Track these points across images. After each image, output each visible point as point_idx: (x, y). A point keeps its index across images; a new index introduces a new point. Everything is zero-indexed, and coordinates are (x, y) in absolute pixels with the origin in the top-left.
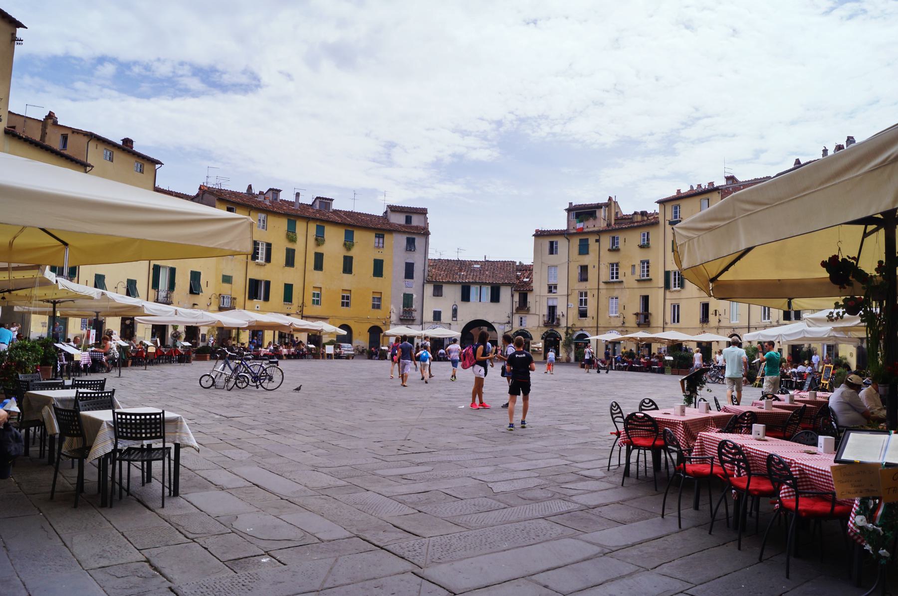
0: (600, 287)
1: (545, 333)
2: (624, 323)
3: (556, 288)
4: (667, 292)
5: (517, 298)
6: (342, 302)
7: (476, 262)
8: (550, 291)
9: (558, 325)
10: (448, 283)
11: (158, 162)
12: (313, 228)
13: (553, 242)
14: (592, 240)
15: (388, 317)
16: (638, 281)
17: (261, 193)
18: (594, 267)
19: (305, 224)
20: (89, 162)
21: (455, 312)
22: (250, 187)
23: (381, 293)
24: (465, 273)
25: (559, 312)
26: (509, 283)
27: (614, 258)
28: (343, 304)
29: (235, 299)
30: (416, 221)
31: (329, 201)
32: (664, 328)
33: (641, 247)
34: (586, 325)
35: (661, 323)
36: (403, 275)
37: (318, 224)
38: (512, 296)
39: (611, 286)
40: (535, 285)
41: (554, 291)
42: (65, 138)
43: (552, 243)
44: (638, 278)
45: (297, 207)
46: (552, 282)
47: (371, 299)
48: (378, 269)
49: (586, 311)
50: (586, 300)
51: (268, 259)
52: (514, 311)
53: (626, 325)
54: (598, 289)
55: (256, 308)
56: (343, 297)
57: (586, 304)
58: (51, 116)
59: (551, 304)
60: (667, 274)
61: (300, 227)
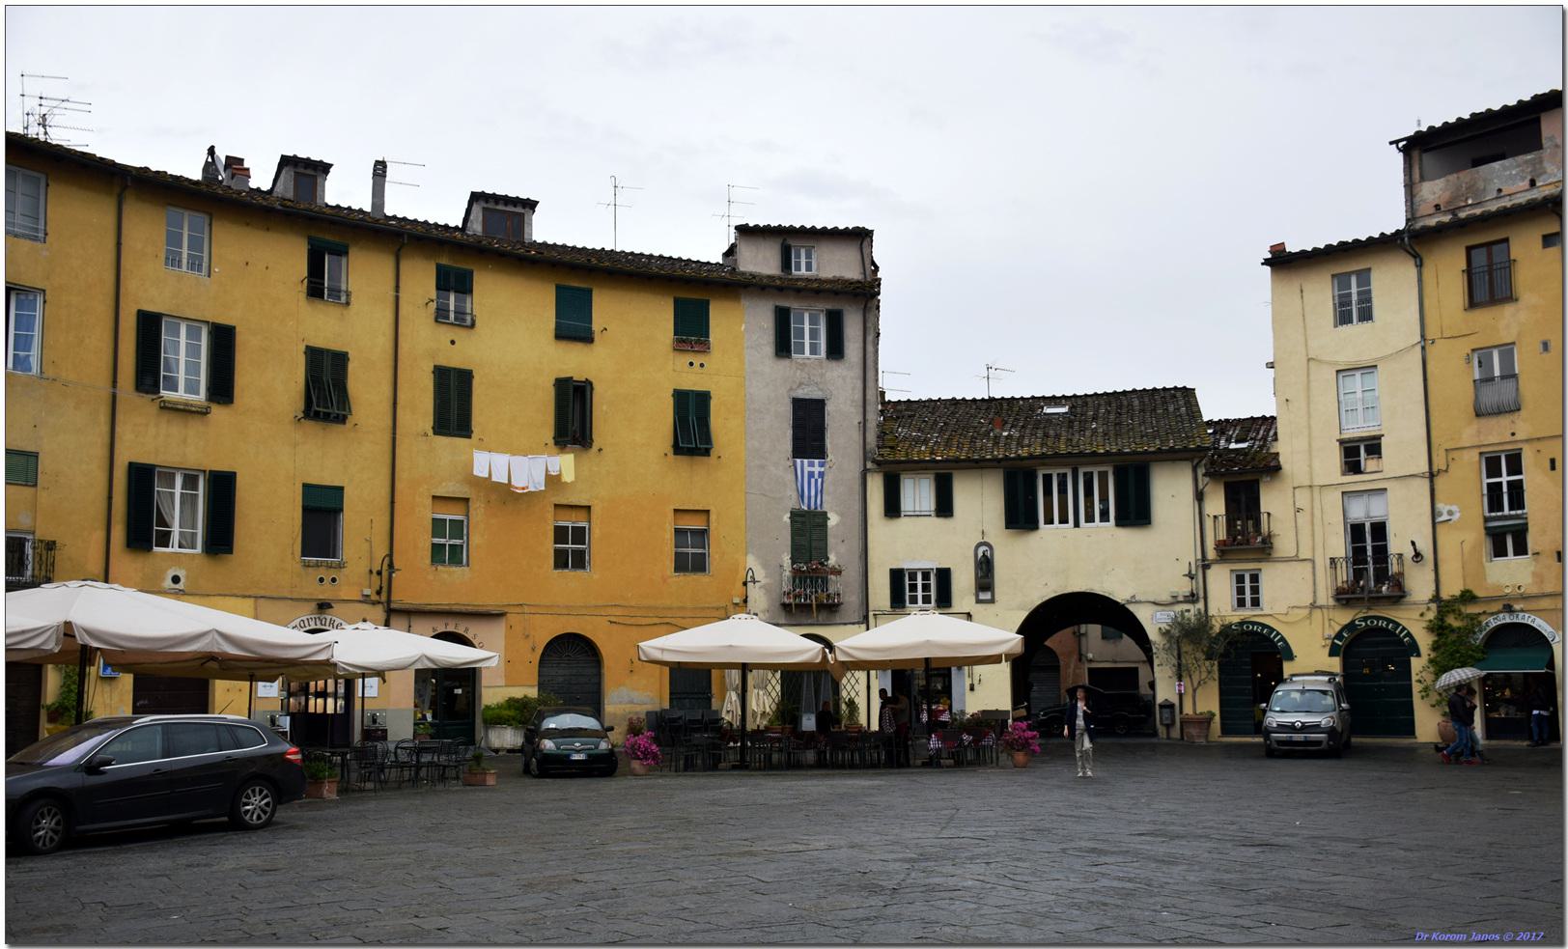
1: (1345, 628)
3: (1374, 447)
6: (557, 552)
7: (1054, 400)
8: (1352, 466)
15: (737, 600)
21: (985, 570)
24: (1015, 433)
25: (1397, 544)
26: (1186, 449)
28: (561, 561)
29: (51, 546)
30: (834, 265)
31: (519, 210)
36: (787, 445)
38: (1199, 497)
40: (1287, 448)
41: (1369, 464)
47: (669, 535)
49: (1527, 524)
50: (1517, 489)
51: (222, 387)
52: (1211, 554)
55: (168, 583)
56: (560, 534)
57: (1517, 500)
59: (1358, 512)
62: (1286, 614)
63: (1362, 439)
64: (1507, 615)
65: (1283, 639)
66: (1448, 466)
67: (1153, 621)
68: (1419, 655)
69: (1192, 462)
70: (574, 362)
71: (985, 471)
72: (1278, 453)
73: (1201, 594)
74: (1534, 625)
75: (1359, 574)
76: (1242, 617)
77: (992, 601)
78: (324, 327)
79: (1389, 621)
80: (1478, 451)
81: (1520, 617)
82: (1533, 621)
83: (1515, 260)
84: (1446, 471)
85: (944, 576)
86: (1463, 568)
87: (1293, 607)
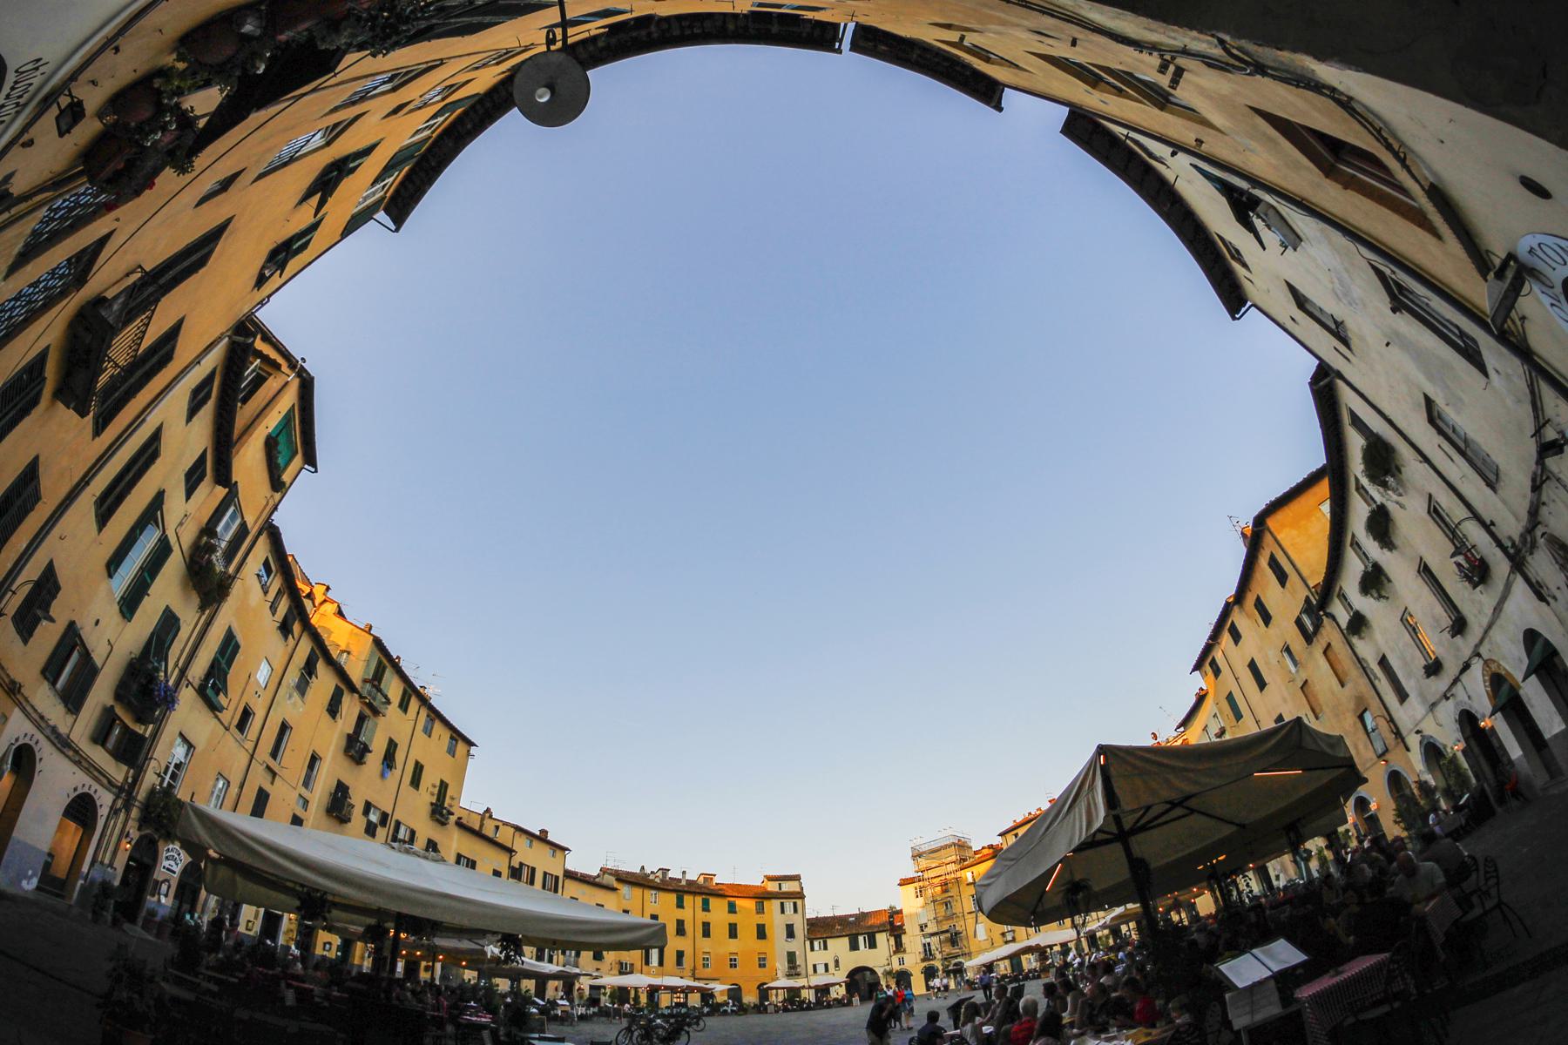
7: (851, 916)
11: (568, 849)
12: (699, 899)
17: (652, 872)
19: (692, 898)
20: (514, 848)
22: (643, 868)
25: (933, 947)
37: (704, 897)
38: (888, 940)
42: (497, 828)
45: (684, 883)
48: (761, 933)
56: (731, 960)
58: (488, 810)
61: (688, 899)
67: (880, 972)
70: (732, 918)
75: (926, 954)
78: (680, 914)
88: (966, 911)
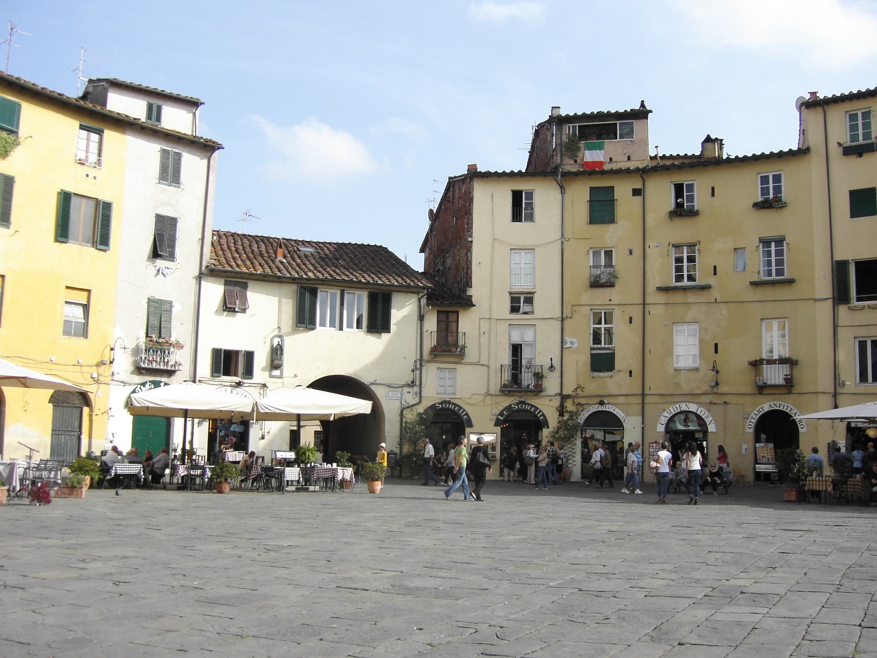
0: (649, 300)
2: (717, 384)
3: (529, 300)
4: (843, 309)
5: (431, 323)
8: (515, 309)
9: (538, 390)
10: (264, 279)
13: (520, 192)
14: (623, 190)
16: (755, 284)
18: (631, 252)
23: (89, 291)
27: (684, 231)
32: (835, 395)
33: (765, 205)
34: (616, 392)
35: (825, 382)
38: (421, 318)
39: (678, 297)
40: (476, 292)
41: (524, 307)
43: (517, 196)
44: (755, 278)
46: (522, 285)
49: (614, 353)
50: (609, 332)
52: (426, 355)
53: (723, 389)
54: (644, 304)
60: (840, 268)
62: (470, 398)
63: (523, 293)
64: (600, 407)
65: (467, 414)
66: (572, 315)
68: (548, 427)
69: (418, 295)
71: (282, 284)
72: (471, 296)
73: (418, 383)
74: (615, 413)
76: (443, 399)
77: (281, 377)
79: (532, 406)
80: (589, 308)
81: (607, 407)
82: (614, 410)
83: (617, 200)
84: (571, 318)
85: (250, 356)
86: (577, 376)
87: (474, 394)
88: (655, 282)
